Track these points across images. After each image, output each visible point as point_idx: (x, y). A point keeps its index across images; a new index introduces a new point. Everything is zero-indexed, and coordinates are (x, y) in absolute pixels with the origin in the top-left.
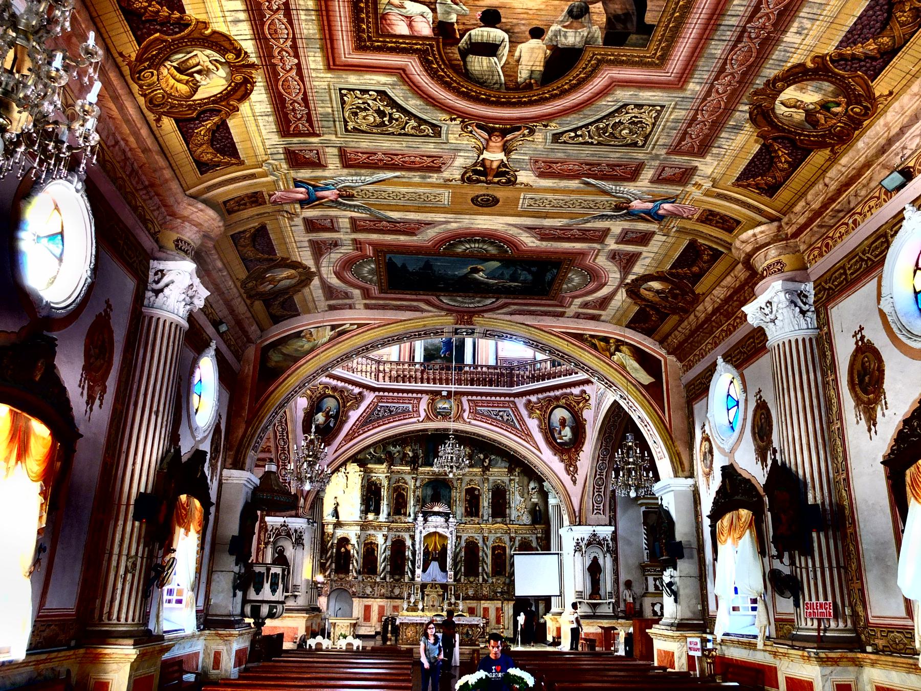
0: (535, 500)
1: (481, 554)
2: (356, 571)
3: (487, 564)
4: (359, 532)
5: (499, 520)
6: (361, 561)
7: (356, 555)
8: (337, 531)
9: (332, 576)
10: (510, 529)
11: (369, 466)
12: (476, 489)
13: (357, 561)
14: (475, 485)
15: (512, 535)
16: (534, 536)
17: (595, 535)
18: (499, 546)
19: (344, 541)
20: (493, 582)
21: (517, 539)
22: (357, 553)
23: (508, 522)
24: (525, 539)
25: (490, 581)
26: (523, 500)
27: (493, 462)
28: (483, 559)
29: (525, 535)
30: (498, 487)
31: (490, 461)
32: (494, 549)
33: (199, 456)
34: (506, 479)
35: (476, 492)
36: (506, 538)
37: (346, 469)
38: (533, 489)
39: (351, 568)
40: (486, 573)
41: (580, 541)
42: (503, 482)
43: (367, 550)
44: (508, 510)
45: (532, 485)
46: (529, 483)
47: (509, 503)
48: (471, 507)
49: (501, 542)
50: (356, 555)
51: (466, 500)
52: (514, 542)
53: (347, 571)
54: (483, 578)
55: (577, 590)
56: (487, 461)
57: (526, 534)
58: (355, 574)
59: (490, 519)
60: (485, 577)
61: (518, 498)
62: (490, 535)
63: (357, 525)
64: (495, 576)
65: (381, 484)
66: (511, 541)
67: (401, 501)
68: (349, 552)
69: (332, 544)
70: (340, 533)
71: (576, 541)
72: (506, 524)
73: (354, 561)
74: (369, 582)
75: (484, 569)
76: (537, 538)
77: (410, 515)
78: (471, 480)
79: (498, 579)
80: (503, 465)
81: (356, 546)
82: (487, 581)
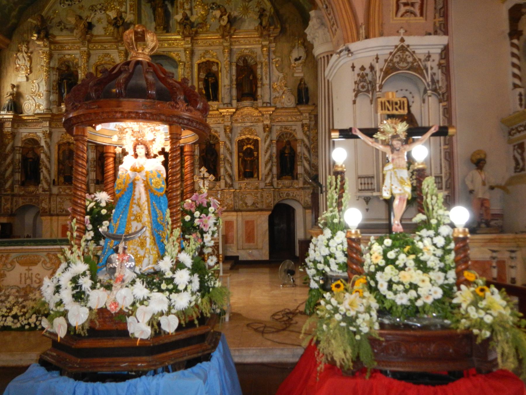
0: (299, 74)
1: (222, 150)
2: (47, 182)
3: (231, 164)
4: (48, 130)
5: (246, 103)
6: (54, 168)
7: (45, 160)
8: (21, 131)
9: (16, 191)
10: (263, 115)
11: (58, 39)
12: (213, 62)
13: (46, 167)
14: (213, 57)
15: (267, 122)
16: (299, 124)
17: (403, 49)
18: (248, 139)
19: (34, 142)
20: (240, 188)
21: (274, 129)
22: (49, 158)
23: (260, 105)
24: (286, 128)
25: (237, 185)
26: (281, 75)
28: (225, 158)
29: (286, 123)
30: (245, 61)
32: (241, 143)
34: (257, 48)
35: (214, 68)
36: (259, 128)
37: (28, 48)
38: (296, 60)
40: (230, 177)
41: (368, 71)
42: (252, 52)
43: (64, 152)
44: (259, 90)
45: (295, 54)
46: (291, 52)
47: (261, 79)
48: (207, 88)
49: (252, 134)
50: (45, 160)
52: (270, 131)
53: (37, 181)
54: (226, 183)
55: (360, 173)
56: (225, 18)
57: (288, 121)
58: (46, 186)
59: (234, 102)
60: (229, 181)
61: (276, 74)
62: (235, 125)
63: (45, 119)
64: (243, 180)
65: (77, 64)
66: (264, 131)
68: (38, 158)
69: (13, 148)
70: (25, 132)
71: (357, 70)
72: (257, 109)
74: (68, 195)
75: (226, 171)
76: (303, 126)
78: (207, 52)
79: (248, 184)
81: (45, 148)
82: (232, 186)
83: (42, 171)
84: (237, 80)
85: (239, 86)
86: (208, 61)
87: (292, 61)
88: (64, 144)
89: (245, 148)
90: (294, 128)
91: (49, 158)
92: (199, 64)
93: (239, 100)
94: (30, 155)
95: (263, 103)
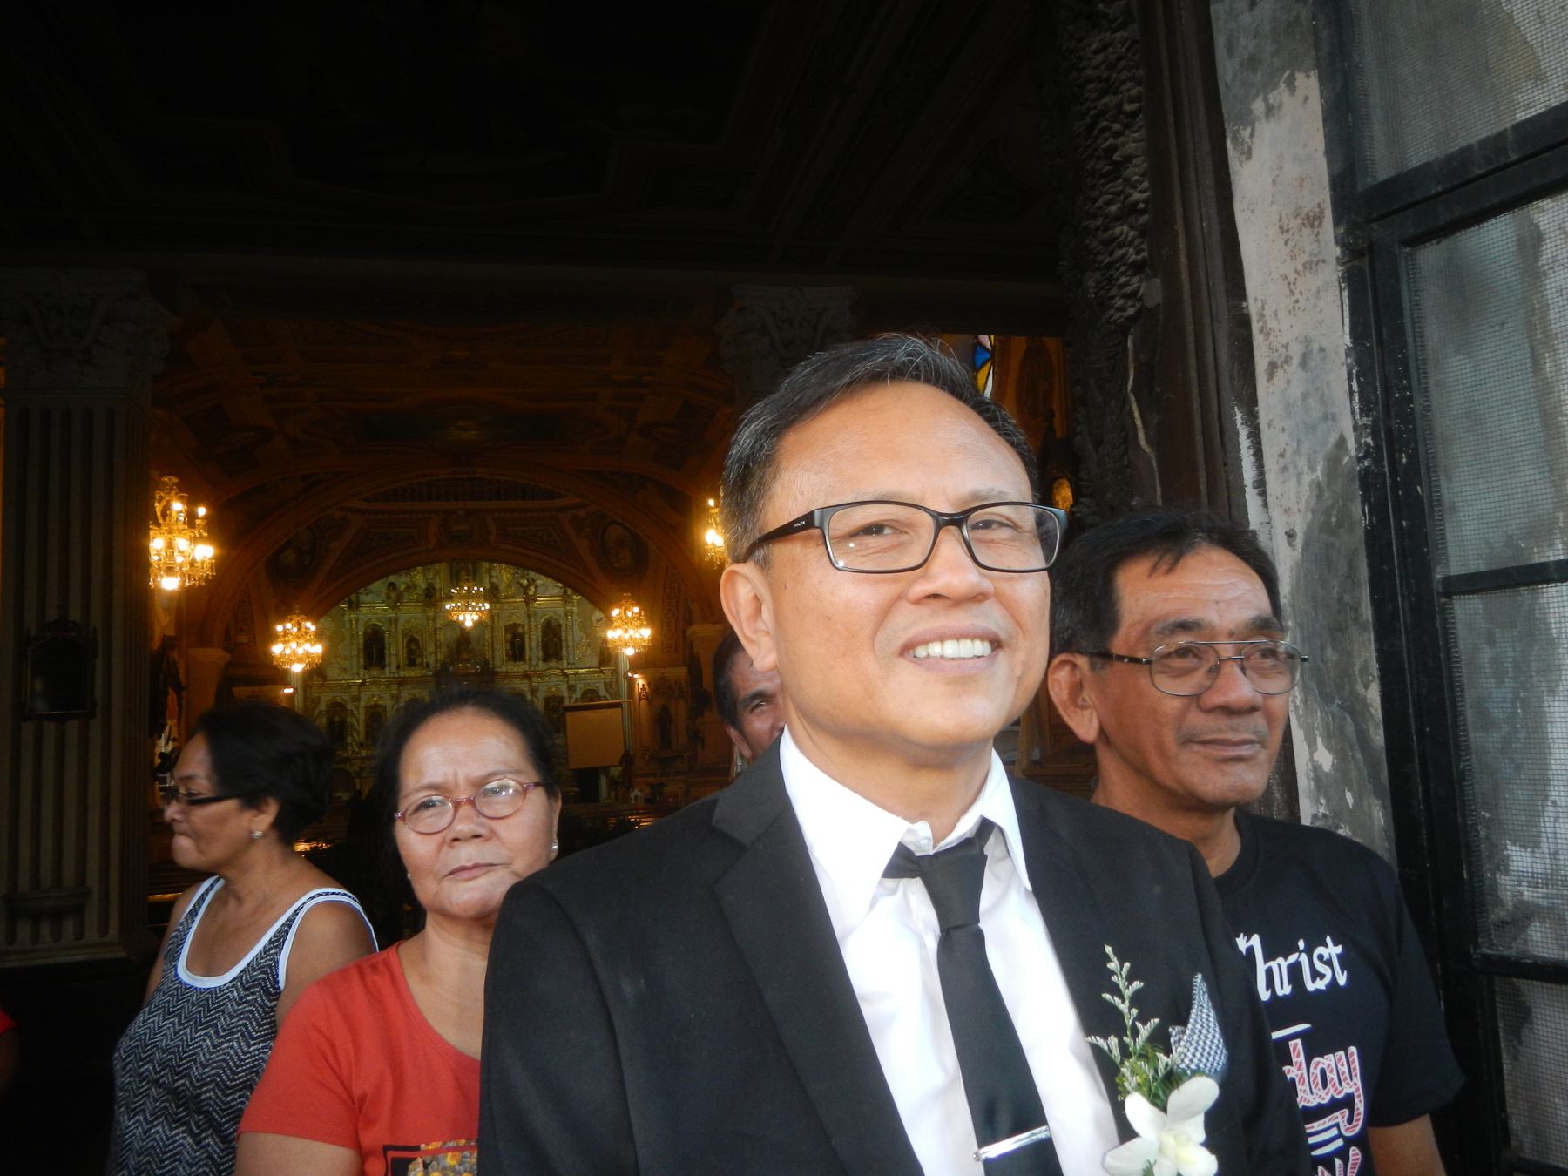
6: (362, 728)
7: (355, 723)
15: (571, 683)
27: (540, 589)
31: (536, 587)
33: (168, 643)
35: (520, 630)
39: (349, 740)
50: (355, 723)
51: (506, 641)
67: (413, 647)
69: (320, 712)
73: (354, 733)
77: (428, 666)
80: (556, 591)
83: (352, 735)
84: (542, 641)
85: (545, 647)
86: (515, 624)
87: (595, 622)
88: (371, 707)
89: (551, 705)
90: (597, 685)
91: (358, 720)
92: (506, 627)
93: (545, 660)
94: (337, 719)
95: (568, 664)
